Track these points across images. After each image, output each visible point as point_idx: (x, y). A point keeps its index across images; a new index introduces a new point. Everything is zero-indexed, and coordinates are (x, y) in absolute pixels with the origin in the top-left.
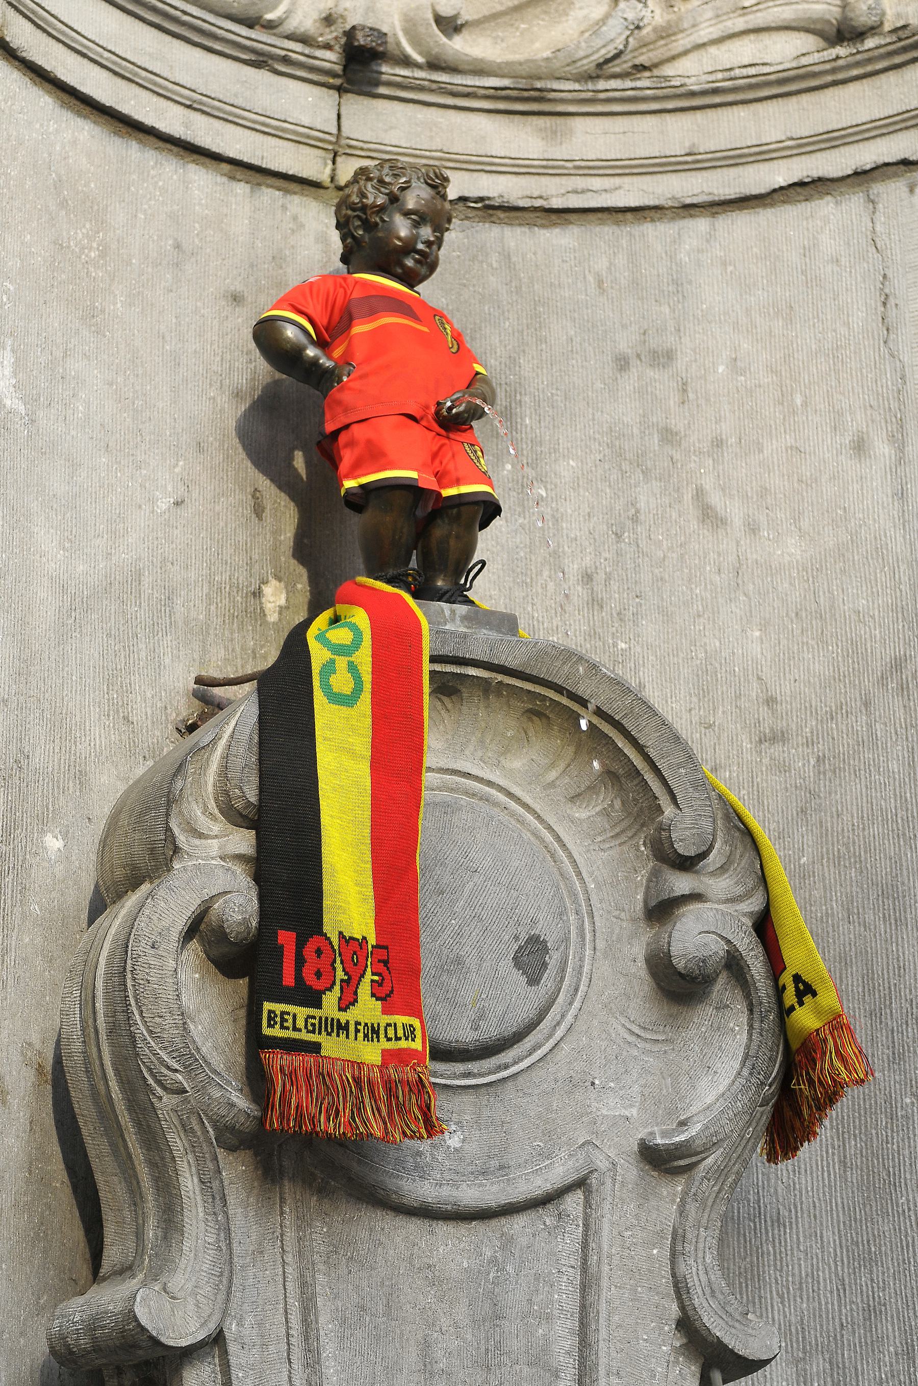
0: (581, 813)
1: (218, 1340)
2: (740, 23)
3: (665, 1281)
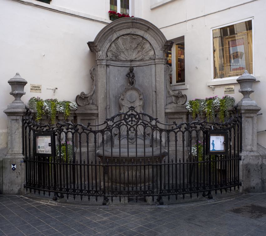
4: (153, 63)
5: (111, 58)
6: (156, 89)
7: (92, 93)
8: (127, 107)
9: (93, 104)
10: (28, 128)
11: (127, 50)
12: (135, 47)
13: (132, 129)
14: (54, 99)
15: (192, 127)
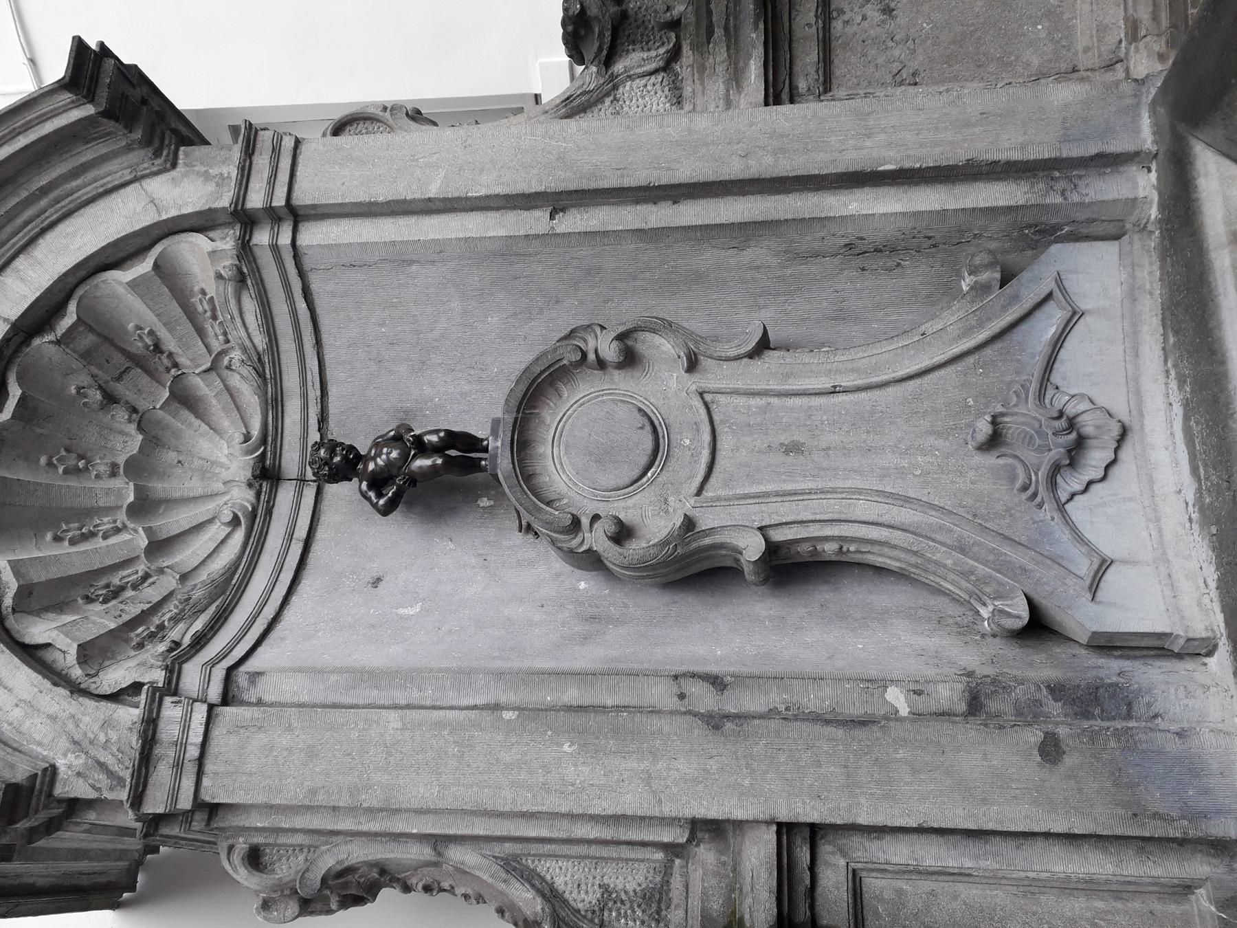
0: (565, 394)
1: (760, 529)
2: (238, 320)
3: (736, 363)
4: (285, 239)
5: (162, 647)
8: (708, 493)
11: (143, 507)
12: (132, 428)
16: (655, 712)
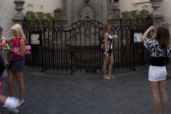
6: (102, 6)
7: (64, 8)
9: (64, 15)
10: (26, 29)
13: (87, 29)
14: (41, 12)
15: (123, 28)
16: (72, 15)
